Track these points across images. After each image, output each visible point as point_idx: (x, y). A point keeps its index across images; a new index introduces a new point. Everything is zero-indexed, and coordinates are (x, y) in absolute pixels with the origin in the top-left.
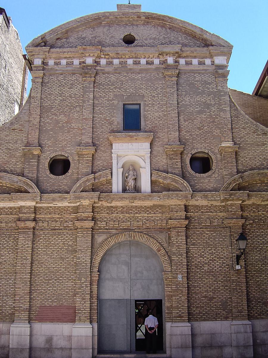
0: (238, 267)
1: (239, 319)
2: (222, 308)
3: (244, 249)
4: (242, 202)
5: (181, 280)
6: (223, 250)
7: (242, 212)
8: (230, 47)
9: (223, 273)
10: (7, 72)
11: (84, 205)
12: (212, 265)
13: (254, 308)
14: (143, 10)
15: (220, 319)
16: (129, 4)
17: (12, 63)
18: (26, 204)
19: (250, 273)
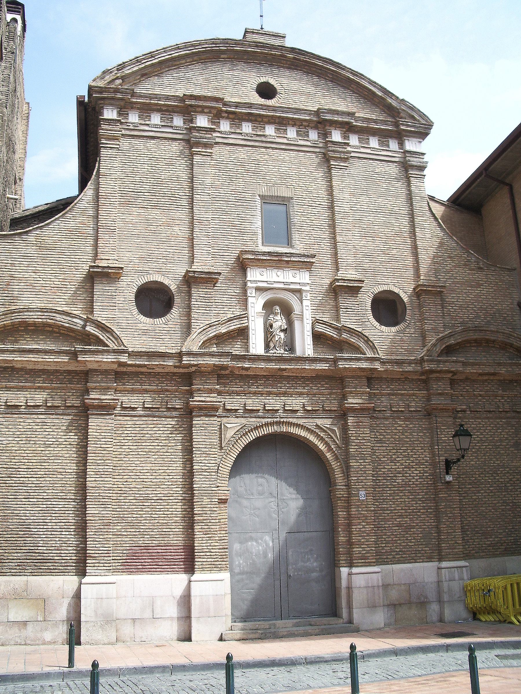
0: (449, 478)
2: (424, 543)
5: (365, 499)
6: (425, 452)
9: (425, 488)
11: (202, 372)
12: (408, 475)
13: (470, 541)
14: (289, 43)
15: (421, 561)
16: (262, 28)
19: (463, 487)
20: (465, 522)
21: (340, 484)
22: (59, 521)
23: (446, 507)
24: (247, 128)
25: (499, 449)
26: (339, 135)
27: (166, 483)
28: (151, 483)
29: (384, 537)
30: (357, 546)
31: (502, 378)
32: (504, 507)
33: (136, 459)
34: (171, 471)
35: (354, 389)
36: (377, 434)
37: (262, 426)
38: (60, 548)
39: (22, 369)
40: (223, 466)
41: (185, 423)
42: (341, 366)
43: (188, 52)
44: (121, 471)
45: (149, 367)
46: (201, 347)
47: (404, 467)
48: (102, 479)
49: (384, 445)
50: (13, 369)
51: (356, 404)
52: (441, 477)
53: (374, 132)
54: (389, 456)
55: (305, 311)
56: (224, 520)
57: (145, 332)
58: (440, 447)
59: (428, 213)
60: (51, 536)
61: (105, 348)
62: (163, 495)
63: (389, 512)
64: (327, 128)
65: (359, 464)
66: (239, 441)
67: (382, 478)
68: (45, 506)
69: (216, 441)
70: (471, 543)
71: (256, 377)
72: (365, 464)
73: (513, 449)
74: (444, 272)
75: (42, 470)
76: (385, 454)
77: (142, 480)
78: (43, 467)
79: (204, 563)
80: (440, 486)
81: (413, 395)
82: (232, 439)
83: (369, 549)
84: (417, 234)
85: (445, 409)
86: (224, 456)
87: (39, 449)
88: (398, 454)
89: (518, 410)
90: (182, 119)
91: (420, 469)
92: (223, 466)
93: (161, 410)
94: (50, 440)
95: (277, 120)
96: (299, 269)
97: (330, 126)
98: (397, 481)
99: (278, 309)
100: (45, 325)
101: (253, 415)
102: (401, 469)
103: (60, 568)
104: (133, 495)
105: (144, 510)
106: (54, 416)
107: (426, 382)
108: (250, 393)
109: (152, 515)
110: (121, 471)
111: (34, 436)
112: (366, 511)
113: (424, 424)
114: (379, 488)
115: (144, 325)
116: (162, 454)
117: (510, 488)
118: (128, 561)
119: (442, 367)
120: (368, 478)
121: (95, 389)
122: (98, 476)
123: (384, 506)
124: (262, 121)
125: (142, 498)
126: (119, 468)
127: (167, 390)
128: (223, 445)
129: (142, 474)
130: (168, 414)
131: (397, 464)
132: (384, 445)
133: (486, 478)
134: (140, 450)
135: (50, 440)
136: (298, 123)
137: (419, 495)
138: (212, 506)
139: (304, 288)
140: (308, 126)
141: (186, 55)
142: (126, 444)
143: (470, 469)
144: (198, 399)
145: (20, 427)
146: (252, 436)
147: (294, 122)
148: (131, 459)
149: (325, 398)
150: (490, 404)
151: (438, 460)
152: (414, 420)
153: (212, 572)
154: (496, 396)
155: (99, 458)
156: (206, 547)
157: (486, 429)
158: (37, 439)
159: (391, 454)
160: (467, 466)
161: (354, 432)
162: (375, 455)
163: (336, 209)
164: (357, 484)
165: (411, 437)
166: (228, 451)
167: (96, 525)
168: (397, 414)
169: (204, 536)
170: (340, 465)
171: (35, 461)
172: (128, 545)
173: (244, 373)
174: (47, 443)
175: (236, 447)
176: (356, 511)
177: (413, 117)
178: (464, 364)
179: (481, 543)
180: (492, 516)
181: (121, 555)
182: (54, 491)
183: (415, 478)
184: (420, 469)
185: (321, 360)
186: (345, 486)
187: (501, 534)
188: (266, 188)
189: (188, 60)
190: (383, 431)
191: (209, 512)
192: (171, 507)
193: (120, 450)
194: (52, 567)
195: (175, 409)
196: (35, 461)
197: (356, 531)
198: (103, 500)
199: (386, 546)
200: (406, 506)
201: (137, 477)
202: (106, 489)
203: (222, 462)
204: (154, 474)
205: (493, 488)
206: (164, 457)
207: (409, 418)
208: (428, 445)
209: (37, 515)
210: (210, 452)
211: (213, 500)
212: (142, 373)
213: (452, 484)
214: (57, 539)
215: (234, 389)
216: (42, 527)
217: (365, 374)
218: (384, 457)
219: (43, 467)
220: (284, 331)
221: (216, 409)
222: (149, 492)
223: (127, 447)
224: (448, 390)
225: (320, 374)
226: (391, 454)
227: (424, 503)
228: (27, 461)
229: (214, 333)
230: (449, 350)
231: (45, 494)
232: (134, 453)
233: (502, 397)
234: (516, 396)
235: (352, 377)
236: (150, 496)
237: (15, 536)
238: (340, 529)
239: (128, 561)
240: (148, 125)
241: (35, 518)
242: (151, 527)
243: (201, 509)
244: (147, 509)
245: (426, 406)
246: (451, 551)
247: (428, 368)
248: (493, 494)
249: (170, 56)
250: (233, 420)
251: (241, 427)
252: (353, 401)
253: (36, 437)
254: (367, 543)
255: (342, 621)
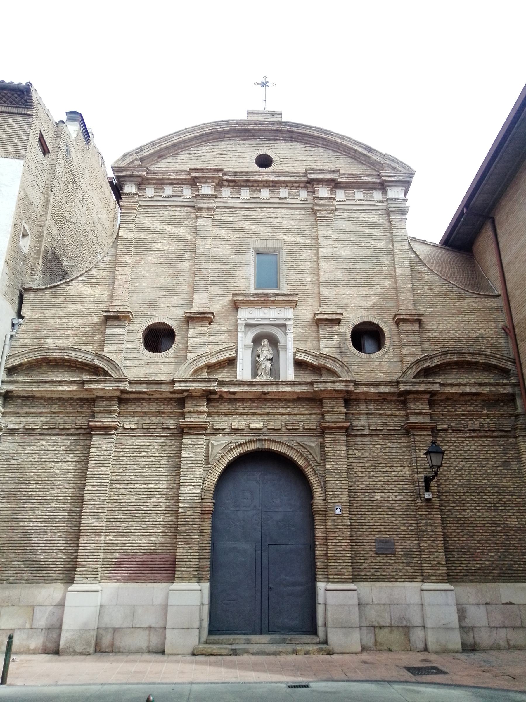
0: (428, 495)
1: (433, 581)
2: (405, 561)
3: (439, 467)
4: (431, 397)
5: (340, 513)
6: (404, 469)
7: (430, 411)
8: (411, 174)
9: (405, 505)
10: (85, 208)
12: (387, 491)
13: (457, 562)
14: (285, 118)
15: (402, 580)
17: (94, 199)
18: (105, 393)
19: (446, 505)
20: (450, 542)
21: (318, 498)
22: (58, 530)
23: (426, 525)
24: (245, 193)
25: (485, 468)
26: (326, 191)
27: (156, 496)
28: (143, 496)
29: (362, 552)
30: (333, 561)
31: (486, 398)
32: (494, 528)
33: (132, 474)
34: (161, 484)
35: (331, 410)
36: (355, 451)
37: (246, 443)
38: (56, 556)
39: (42, 398)
40: (208, 480)
41: (177, 441)
42: (317, 389)
43: (197, 134)
44: (117, 485)
45: (149, 393)
46: (192, 375)
47: (382, 483)
48: (98, 492)
49: (362, 461)
50: (34, 397)
51: (332, 422)
52: (420, 494)
53: (359, 186)
54: (367, 473)
55: (288, 342)
56: (207, 531)
57: (148, 365)
58: (418, 464)
59: (408, 252)
60: (50, 545)
61: (108, 378)
62: (153, 507)
63: (367, 527)
64: (315, 186)
65: (335, 479)
66: (224, 457)
67: (360, 494)
68: (47, 517)
69: (202, 457)
70: (458, 565)
71: (242, 400)
72: (341, 479)
73: (502, 468)
74: (424, 303)
75: (49, 484)
76: (363, 470)
77: (135, 492)
78: (50, 482)
79: (183, 573)
80: (419, 503)
81: (392, 415)
82: (218, 455)
83: (345, 564)
84: (397, 270)
85: (423, 428)
86: (210, 471)
87: (49, 465)
88: (377, 470)
89: (505, 429)
90: (190, 190)
91: (399, 486)
92: (208, 480)
93: (157, 430)
94: (59, 457)
95: (271, 184)
96: (283, 307)
97: (318, 184)
98: (376, 497)
99: (265, 342)
100: (64, 361)
101: (238, 433)
102: (380, 486)
103: (54, 575)
104: (126, 506)
105: (135, 520)
106: (64, 437)
107: (404, 403)
108: (236, 414)
109: (142, 525)
110: (117, 485)
111: (45, 454)
112: (342, 525)
113: (404, 441)
114: (357, 503)
115: (148, 358)
116: (155, 469)
117: (500, 508)
118: (116, 569)
119: (417, 388)
120: (344, 493)
121: (100, 413)
122: (95, 489)
123: (362, 521)
124: (258, 186)
125: (134, 509)
126: (116, 482)
127: (164, 413)
128: (210, 461)
129: (136, 487)
130: (164, 433)
131: (376, 480)
132: (362, 461)
133: (472, 497)
134: (135, 466)
135: (59, 457)
136: (289, 185)
137: (398, 511)
138: (194, 517)
139: (288, 323)
140: (299, 187)
141: (196, 137)
142: (124, 460)
143: (453, 487)
144: (191, 419)
145: (34, 447)
146: (236, 453)
147: (287, 184)
148: (127, 474)
149: (305, 418)
150: (474, 423)
151: (416, 477)
152: (392, 438)
153: (191, 581)
154: (480, 416)
155: (97, 473)
156: (186, 557)
157: (470, 448)
158: (47, 457)
159: (369, 470)
160: (450, 484)
161: (330, 449)
162: (353, 471)
163: (320, 254)
164: (333, 499)
165: (390, 454)
166: (213, 466)
167: (89, 534)
168: (375, 433)
169: (185, 546)
170: (319, 480)
171: (44, 476)
172: (117, 554)
173: (232, 396)
174: (56, 460)
175: (222, 462)
176: (332, 525)
177: (394, 169)
178: (441, 385)
179: (469, 565)
180: (480, 537)
181: (110, 563)
182: (57, 503)
183: (395, 494)
184: (399, 486)
185: (300, 384)
186: (323, 500)
187: (492, 557)
188: (259, 241)
189: (198, 142)
190: (361, 448)
191: (191, 523)
192: (159, 517)
193: (119, 466)
194: (46, 575)
195: (169, 429)
196: (44, 476)
197: (332, 545)
198: (97, 511)
199: (364, 563)
200: (385, 522)
201: (132, 490)
202: (100, 500)
203: (207, 476)
204: (146, 487)
205: (480, 508)
206: (157, 471)
207: (387, 437)
208: (408, 462)
209: (39, 525)
210: (196, 467)
211: (196, 512)
212: (143, 399)
213: (433, 501)
214: (54, 548)
215: (222, 411)
216: (42, 536)
217: (341, 395)
218: (362, 474)
219: (50, 482)
220: (271, 360)
221: (206, 429)
222: (141, 504)
223: (125, 463)
224: (427, 410)
225: (300, 396)
226: (369, 470)
227: (404, 520)
228: (36, 476)
229: (204, 363)
230: (427, 372)
231: (49, 506)
232: (130, 469)
233: (487, 416)
234: (502, 415)
235: (330, 398)
236: (142, 507)
237: (17, 545)
238: (317, 543)
239: (116, 569)
240: (161, 196)
241: (37, 528)
242: (140, 536)
243: (184, 520)
244: (137, 520)
245: (405, 425)
246: (434, 571)
247: (402, 389)
248: (480, 514)
249: (181, 139)
250: (220, 437)
251: (226, 444)
252: (329, 419)
253: (47, 455)
254: (343, 558)
255: (318, 640)
